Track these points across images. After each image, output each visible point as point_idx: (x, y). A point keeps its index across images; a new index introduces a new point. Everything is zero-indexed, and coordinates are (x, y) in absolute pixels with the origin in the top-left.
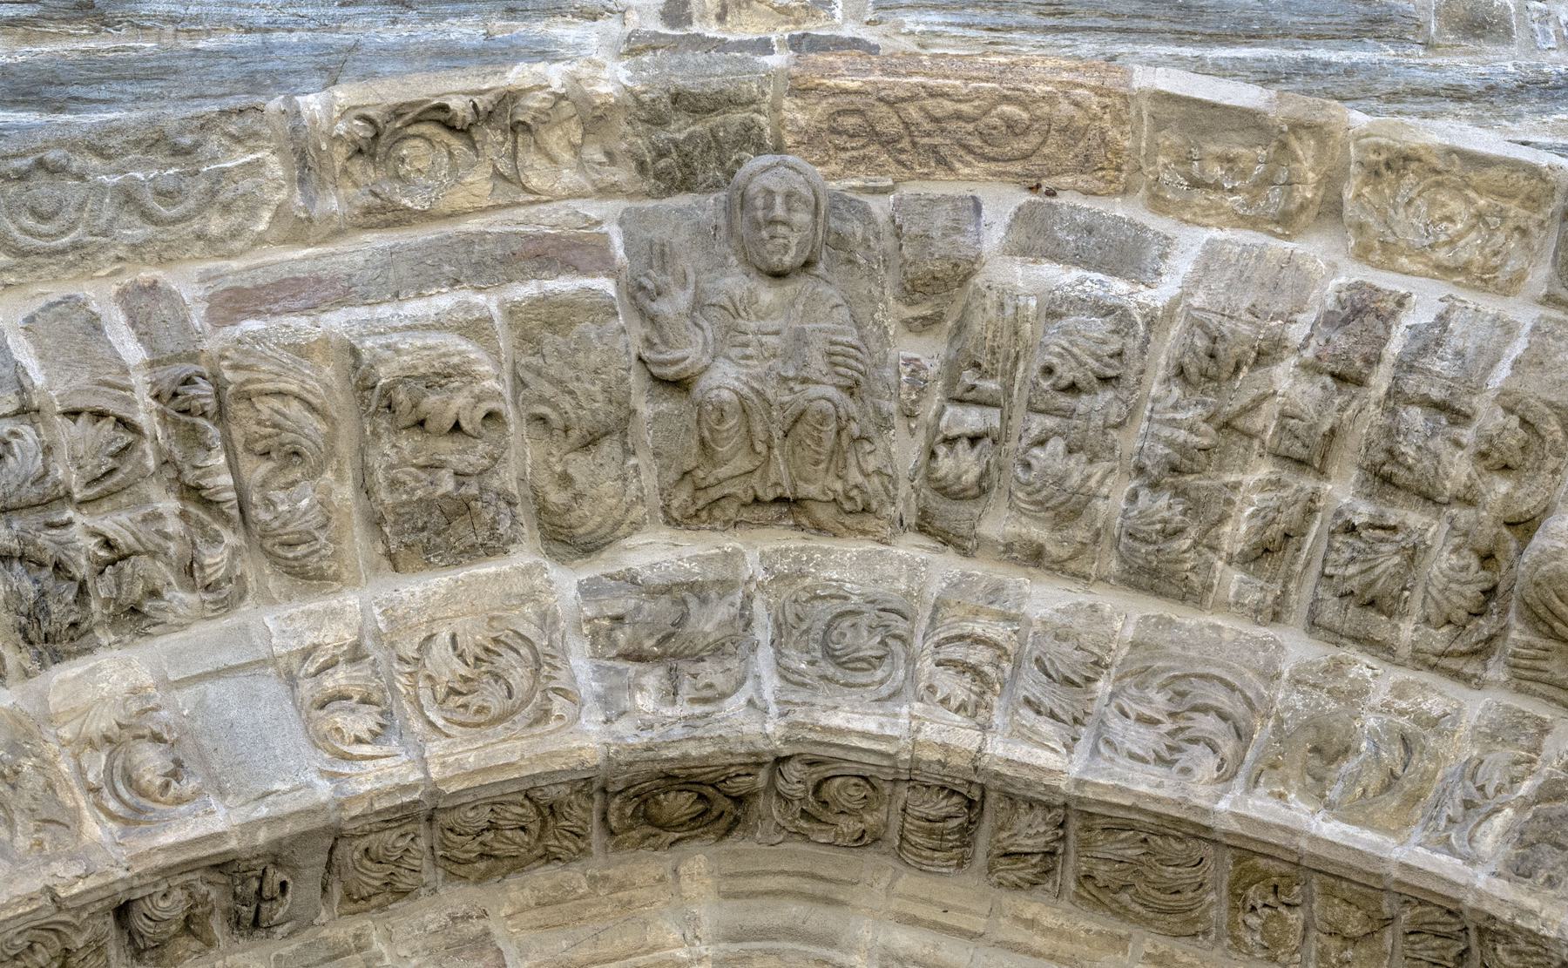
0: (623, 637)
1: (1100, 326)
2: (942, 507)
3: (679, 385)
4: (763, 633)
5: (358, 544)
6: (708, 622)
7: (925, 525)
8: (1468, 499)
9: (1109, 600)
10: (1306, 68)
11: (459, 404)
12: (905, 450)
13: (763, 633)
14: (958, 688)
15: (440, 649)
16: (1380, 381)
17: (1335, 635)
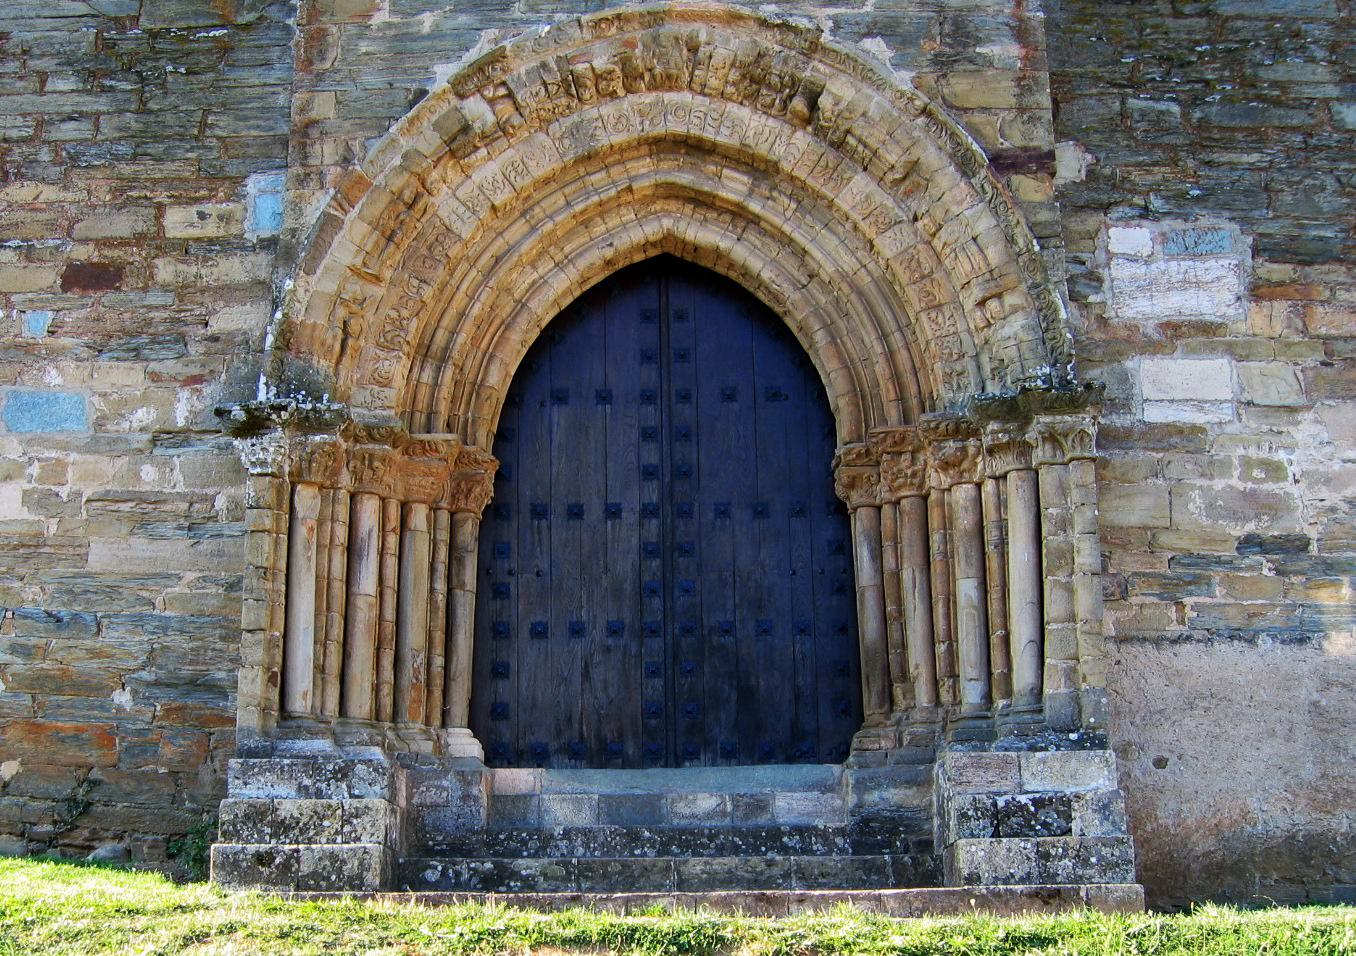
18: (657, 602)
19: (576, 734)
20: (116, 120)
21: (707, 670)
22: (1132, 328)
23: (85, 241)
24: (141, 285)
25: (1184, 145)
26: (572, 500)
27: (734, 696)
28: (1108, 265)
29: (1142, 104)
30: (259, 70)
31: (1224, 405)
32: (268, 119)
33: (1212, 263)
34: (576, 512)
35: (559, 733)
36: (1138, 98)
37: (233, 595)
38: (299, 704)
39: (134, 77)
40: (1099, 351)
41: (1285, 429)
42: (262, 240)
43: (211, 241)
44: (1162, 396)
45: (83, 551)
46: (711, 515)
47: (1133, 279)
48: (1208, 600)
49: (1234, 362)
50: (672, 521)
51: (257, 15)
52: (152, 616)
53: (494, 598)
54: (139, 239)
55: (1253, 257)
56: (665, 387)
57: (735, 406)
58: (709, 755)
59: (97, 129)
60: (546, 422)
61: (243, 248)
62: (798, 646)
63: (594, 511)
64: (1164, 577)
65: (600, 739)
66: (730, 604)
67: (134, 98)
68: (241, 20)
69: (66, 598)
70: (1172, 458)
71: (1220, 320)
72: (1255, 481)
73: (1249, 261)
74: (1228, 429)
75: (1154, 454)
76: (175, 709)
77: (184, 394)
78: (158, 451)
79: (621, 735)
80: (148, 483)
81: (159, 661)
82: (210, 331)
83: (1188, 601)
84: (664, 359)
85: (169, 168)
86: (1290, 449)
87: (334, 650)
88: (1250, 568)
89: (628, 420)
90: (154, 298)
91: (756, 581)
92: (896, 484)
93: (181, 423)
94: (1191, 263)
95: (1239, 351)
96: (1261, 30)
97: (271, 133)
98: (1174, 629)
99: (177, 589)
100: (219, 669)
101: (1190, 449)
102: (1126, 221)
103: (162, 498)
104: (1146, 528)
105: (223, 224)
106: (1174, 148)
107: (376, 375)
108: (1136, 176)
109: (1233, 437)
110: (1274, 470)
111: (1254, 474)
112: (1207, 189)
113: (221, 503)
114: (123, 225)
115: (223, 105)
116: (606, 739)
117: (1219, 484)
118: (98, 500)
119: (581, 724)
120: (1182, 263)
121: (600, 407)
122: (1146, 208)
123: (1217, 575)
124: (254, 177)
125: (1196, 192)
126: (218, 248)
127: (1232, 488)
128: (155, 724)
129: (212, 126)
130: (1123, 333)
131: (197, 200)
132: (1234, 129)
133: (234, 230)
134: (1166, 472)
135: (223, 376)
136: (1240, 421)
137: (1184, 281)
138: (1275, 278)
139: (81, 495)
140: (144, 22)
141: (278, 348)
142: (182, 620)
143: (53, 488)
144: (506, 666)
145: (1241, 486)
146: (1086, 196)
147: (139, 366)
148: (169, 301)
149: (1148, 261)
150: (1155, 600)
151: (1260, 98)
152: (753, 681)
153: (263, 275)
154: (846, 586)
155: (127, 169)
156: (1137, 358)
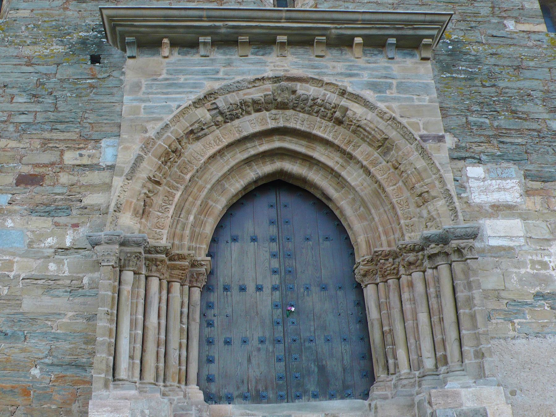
0: (272, 118)
1: (306, 96)
2: (290, 85)
3: (276, 100)
4: (281, 117)
5: (253, 112)
6: (278, 117)
7: (293, 109)
8: (331, 110)
9: (305, 115)
10: (321, 72)
11: (261, 102)
12: (291, 104)
13: (281, 117)
14: (295, 122)
15: (259, 119)
16: (325, 101)
17: (321, 118)
18: (280, 328)
19: (246, 388)
20: (44, 115)
21: (304, 358)
22: (480, 206)
23: (28, 164)
24: (52, 184)
25: (493, 135)
26: (241, 283)
27: (316, 370)
28: (468, 182)
29: (475, 119)
30: (108, 96)
31: (521, 238)
32: (111, 116)
33: (509, 181)
34: (243, 289)
35: (238, 388)
36: (473, 117)
37: (90, 323)
38: (122, 373)
39: (53, 98)
40: (468, 216)
41: (546, 248)
42: (108, 166)
43: (84, 166)
44: (495, 235)
45: (19, 302)
46: (302, 290)
47: (479, 187)
48: (524, 321)
49: (522, 221)
50: (286, 292)
51: (108, 75)
52: (51, 333)
53: (207, 327)
54: (52, 164)
55: (525, 179)
56: (280, 234)
57: (311, 243)
58: (306, 397)
59: (35, 118)
60: (229, 249)
61: (99, 170)
62: (343, 346)
63: (251, 288)
64: (505, 311)
65: (258, 391)
66: (312, 329)
67: (53, 106)
68: (99, 76)
69: (10, 324)
70: (502, 260)
71: (515, 204)
72: (537, 269)
73: (523, 181)
74: (524, 248)
75: (495, 259)
76: (61, 377)
77: (70, 232)
78: (57, 257)
79: (266, 389)
80: (52, 271)
81: (54, 354)
82: (82, 204)
83: (516, 321)
84: (279, 224)
85: (66, 136)
86: (550, 255)
87: (139, 346)
88: (540, 306)
89: (264, 249)
90: (58, 190)
91: (323, 318)
92: (386, 274)
93: (68, 244)
94: (500, 181)
95: (524, 216)
96: (516, 93)
97: (113, 122)
98: (512, 333)
99: (64, 320)
100: (83, 358)
101: (510, 257)
102: (473, 165)
104: (495, 290)
105: (90, 159)
106: (489, 136)
107: (158, 225)
108: (474, 146)
109: (526, 251)
110: (545, 265)
111: (536, 267)
112: (503, 152)
113: (85, 281)
114: (46, 158)
115: (91, 110)
116: (259, 391)
117: (523, 271)
118: (28, 279)
119: (248, 384)
120: (497, 181)
121: (252, 243)
122: (480, 159)
123: (526, 309)
124: (104, 139)
125: (500, 153)
127: (528, 272)
128: (51, 384)
129: (86, 118)
130: (477, 209)
131: (79, 149)
132: (510, 129)
133: (95, 161)
134: (500, 266)
135: (88, 224)
136: (528, 245)
137: (499, 188)
138: (535, 187)
139: (20, 276)
140: (58, 76)
141: (115, 211)
142: (65, 334)
144: (213, 357)
145: (531, 272)
146: (456, 155)
147: (50, 219)
148: (65, 191)
149: (484, 180)
150: (502, 321)
151: (519, 118)
152: (324, 362)
153: (107, 180)
154: (363, 321)
155: (47, 135)
156: (483, 219)
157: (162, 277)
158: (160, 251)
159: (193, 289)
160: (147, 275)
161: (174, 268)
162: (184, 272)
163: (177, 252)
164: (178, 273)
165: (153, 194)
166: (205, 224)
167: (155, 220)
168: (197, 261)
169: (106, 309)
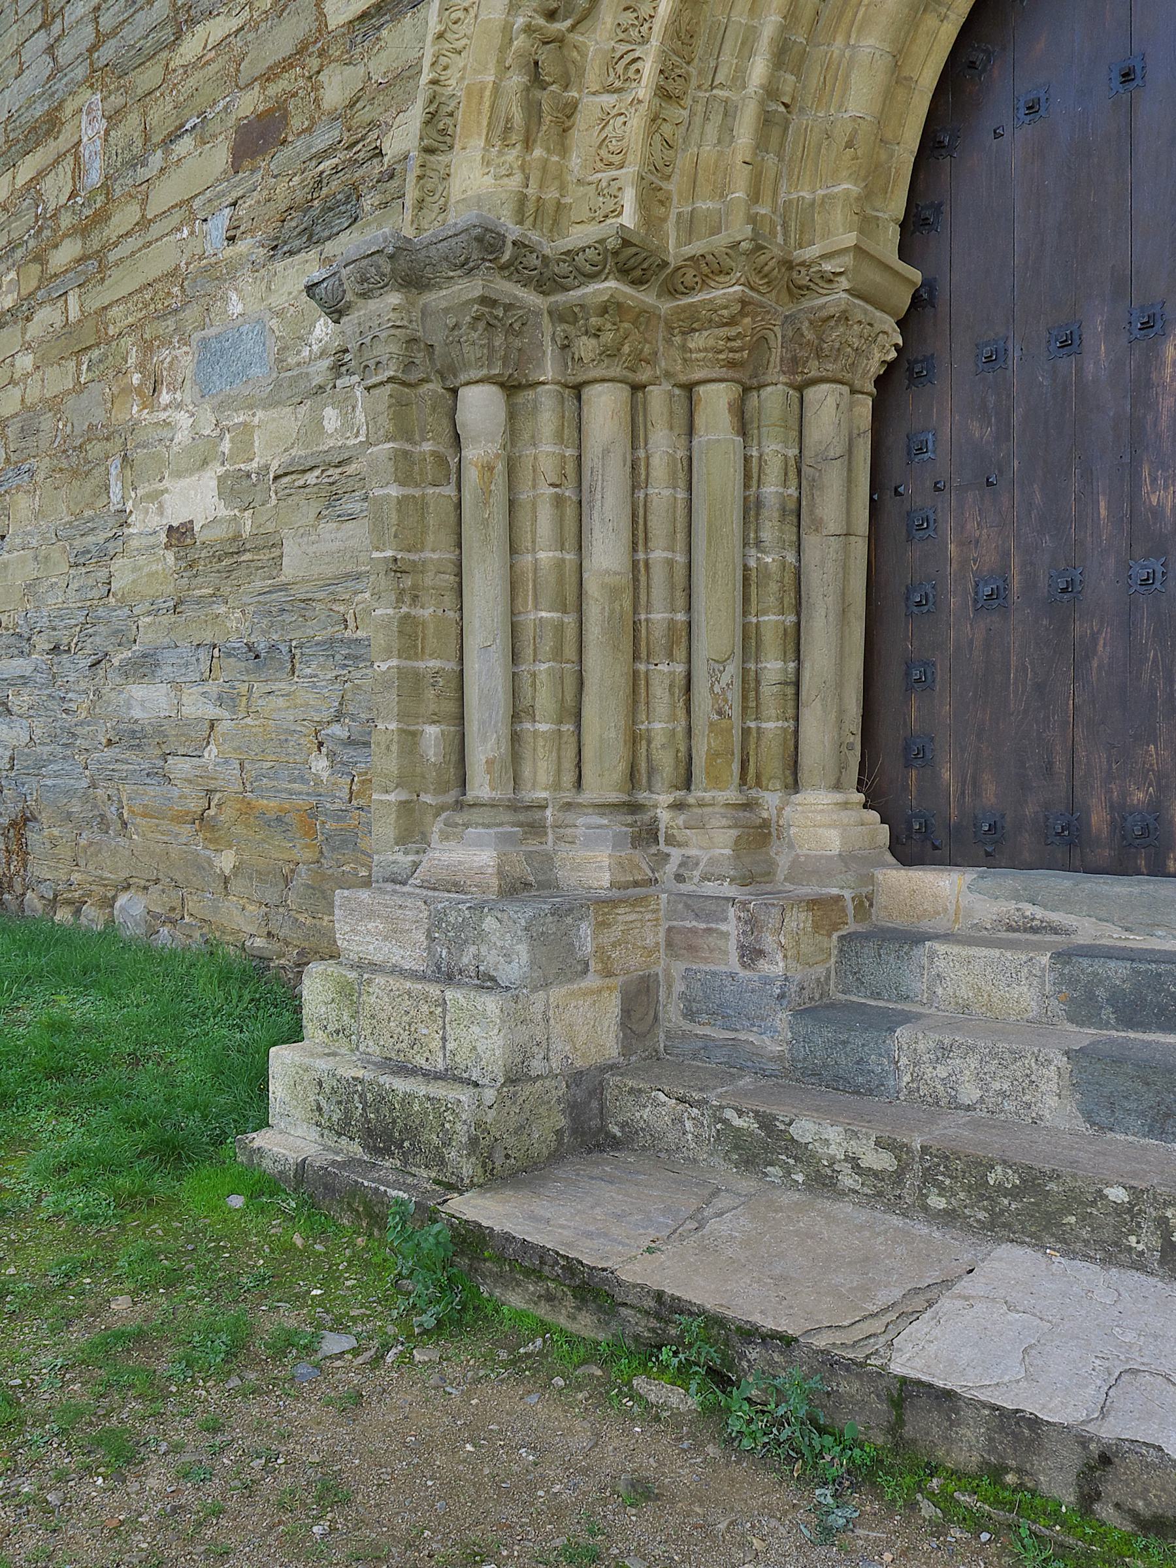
103: (346, 456)
107: (603, 152)
118: (286, 474)
126: (387, 17)
143: (242, 466)
157: (643, 376)
158: (588, 268)
159: (811, 393)
160: (572, 380)
161: (691, 323)
162: (732, 331)
163: (689, 250)
164: (711, 342)
165: (568, 23)
166: (847, 76)
167: (594, 137)
168: (802, 264)
169: (389, 553)
